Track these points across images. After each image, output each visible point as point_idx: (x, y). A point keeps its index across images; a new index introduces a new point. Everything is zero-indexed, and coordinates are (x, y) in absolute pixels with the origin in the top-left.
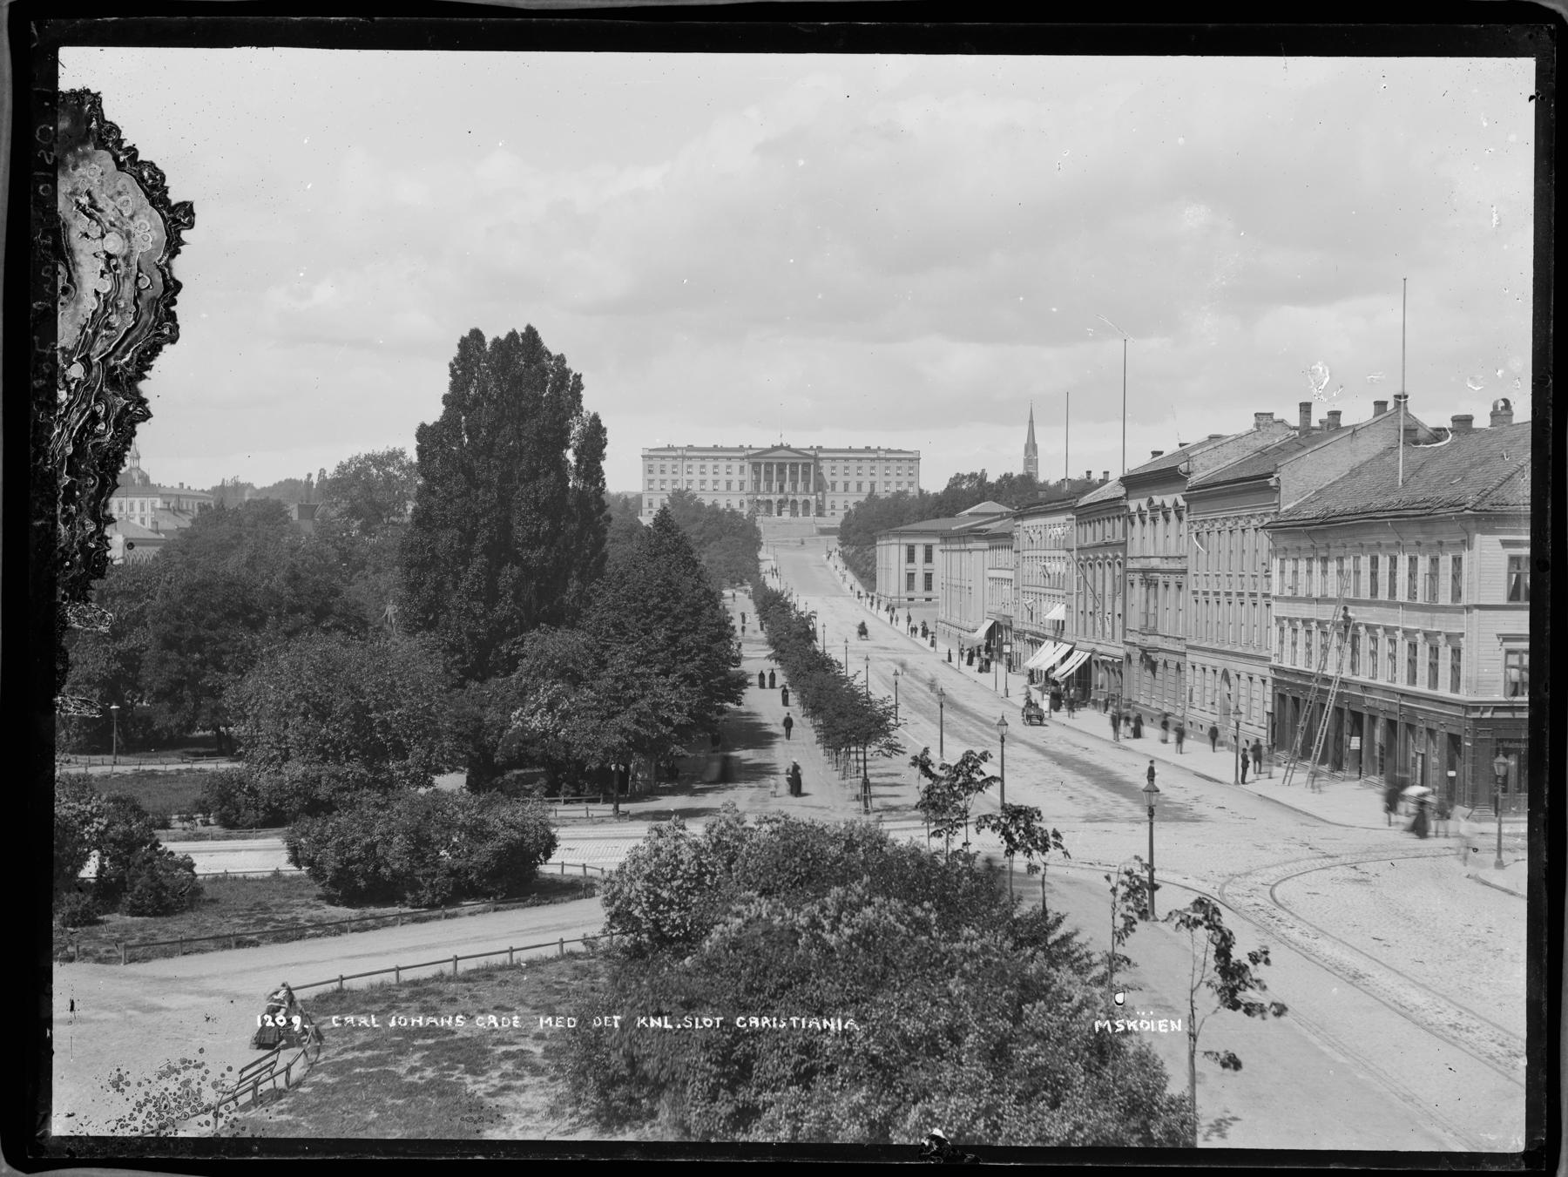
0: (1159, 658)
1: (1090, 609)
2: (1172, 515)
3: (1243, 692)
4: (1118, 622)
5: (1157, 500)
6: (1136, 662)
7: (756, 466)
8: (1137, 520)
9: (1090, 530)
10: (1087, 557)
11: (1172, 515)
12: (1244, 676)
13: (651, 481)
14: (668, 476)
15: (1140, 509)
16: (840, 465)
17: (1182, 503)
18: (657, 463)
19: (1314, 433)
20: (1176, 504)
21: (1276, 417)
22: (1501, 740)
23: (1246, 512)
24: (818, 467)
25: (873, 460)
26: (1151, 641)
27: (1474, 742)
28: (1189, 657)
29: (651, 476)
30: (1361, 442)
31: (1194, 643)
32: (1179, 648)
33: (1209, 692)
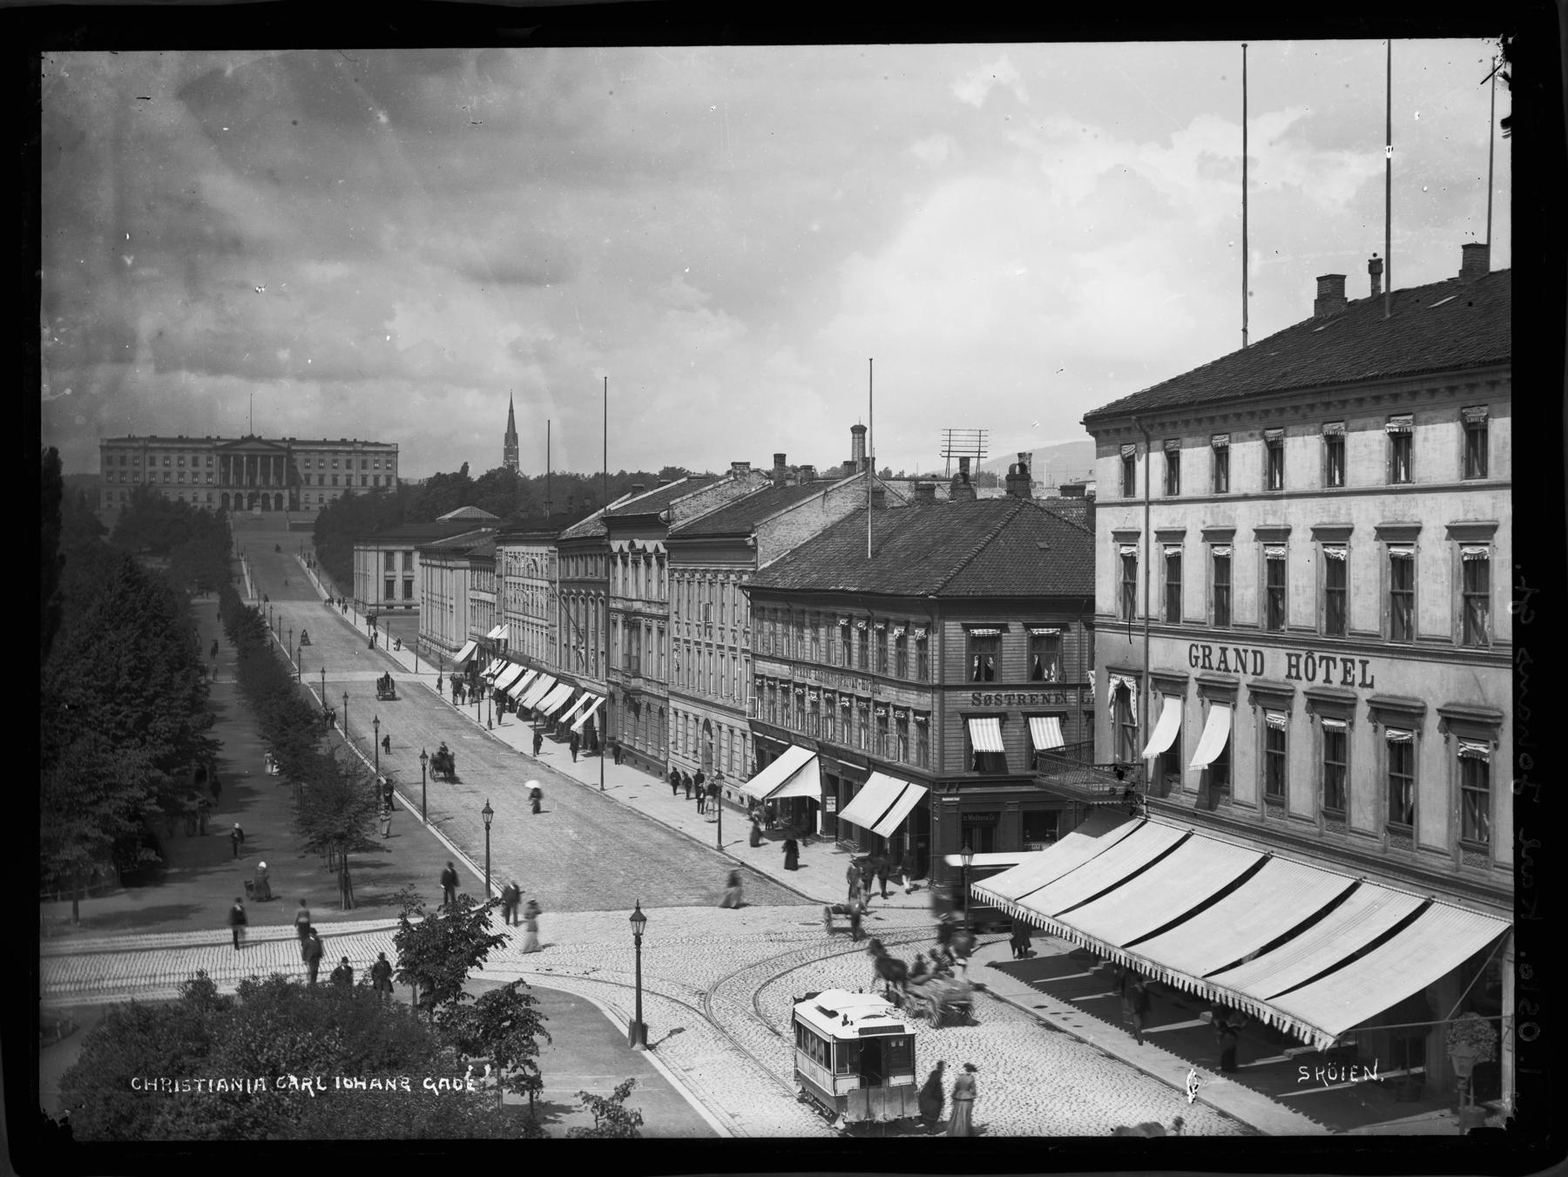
0: (644, 699)
1: (573, 643)
2: (654, 561)
3: (724, 744)
4: (602, 660)
5: (639, 544)
6: (620, 703)
7: (225, 460)
8: (619, 561)
9: (572, 565)
10: (569, 591)
11: (654, 561)
12: (725, 728)
13: (110, 473)
15: (621, 549)
17: (662, 550)
19: (790, 484)
20: (657, 550)
21: (752, 467)
22: (965, 814)
23: (725, 568)
24: (291, 461)
25: (349, 453)
26: (634, 683)
27: (941, 818)
28: (672, 703)
30: (833, 503)
31: (678, 689)
32: (662, 693)
33: (691, 740)
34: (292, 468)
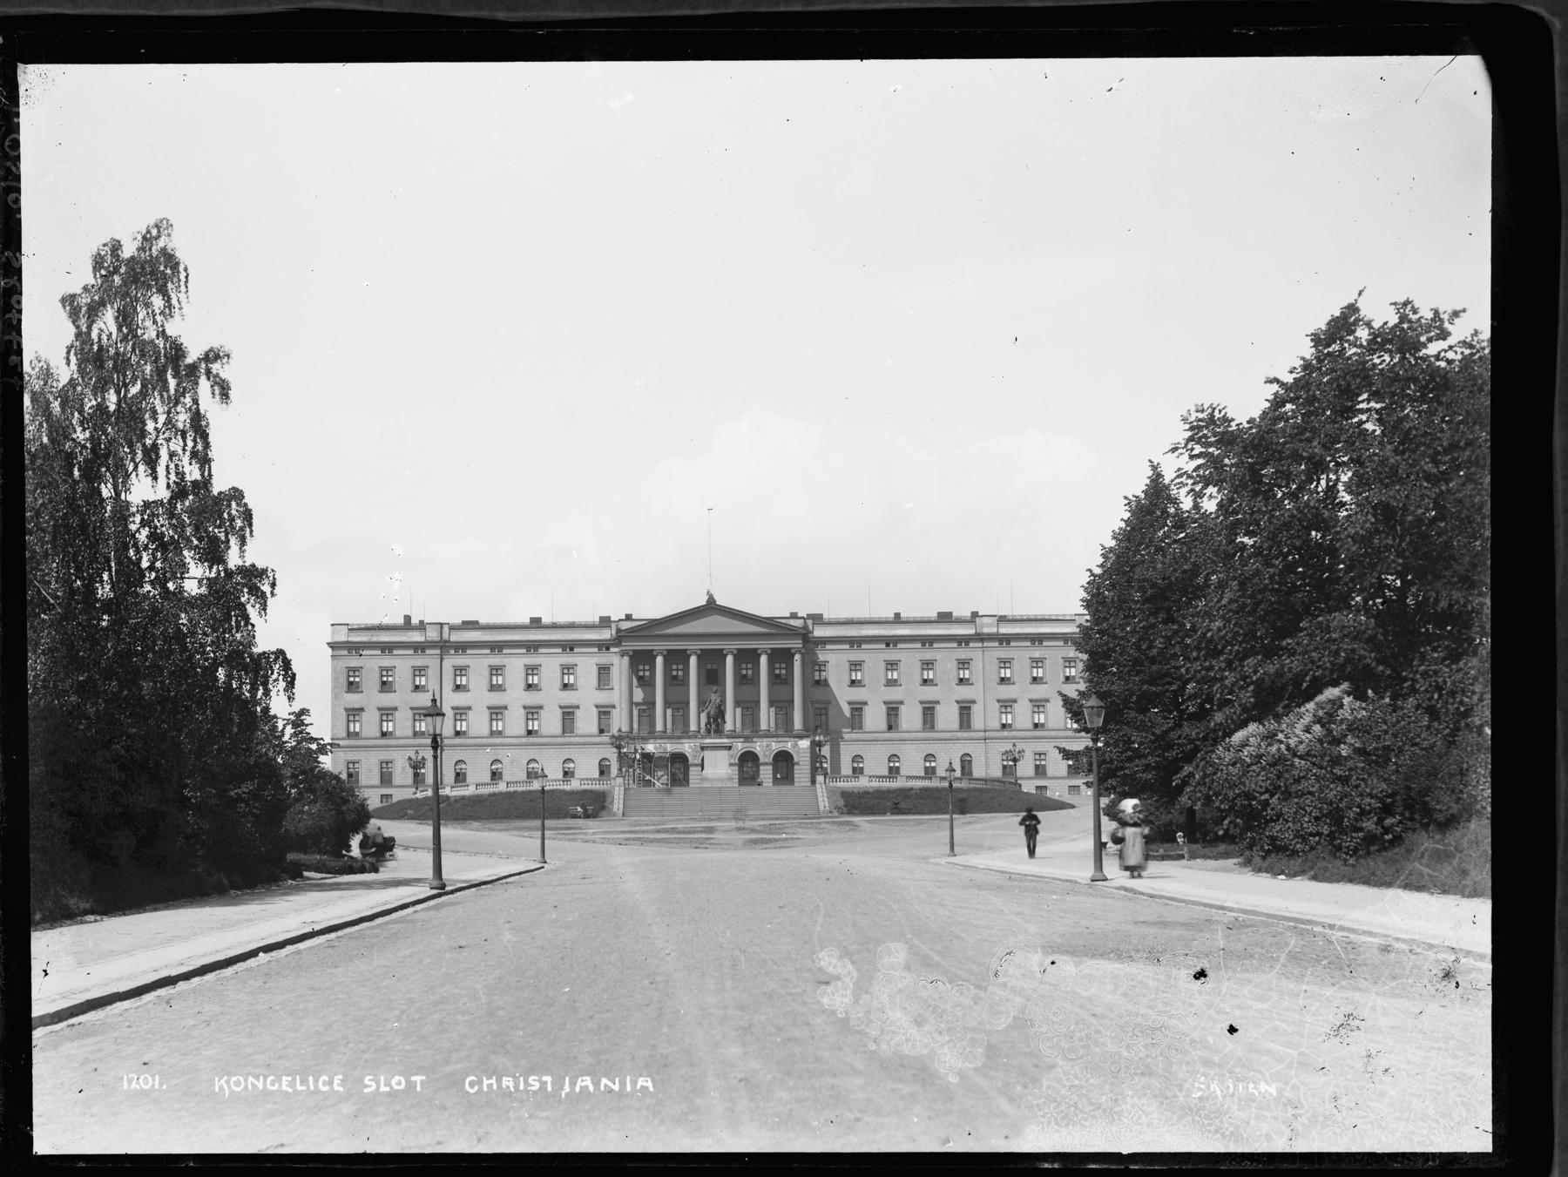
13: (354, 713)
14: (403, 698)
16: (874, 659)
18: (372, 663)
24: (813, 666)
25: (963, 641)
29: (354, 700)
34: (817, 685)
